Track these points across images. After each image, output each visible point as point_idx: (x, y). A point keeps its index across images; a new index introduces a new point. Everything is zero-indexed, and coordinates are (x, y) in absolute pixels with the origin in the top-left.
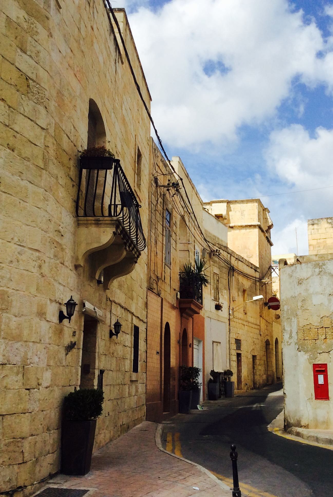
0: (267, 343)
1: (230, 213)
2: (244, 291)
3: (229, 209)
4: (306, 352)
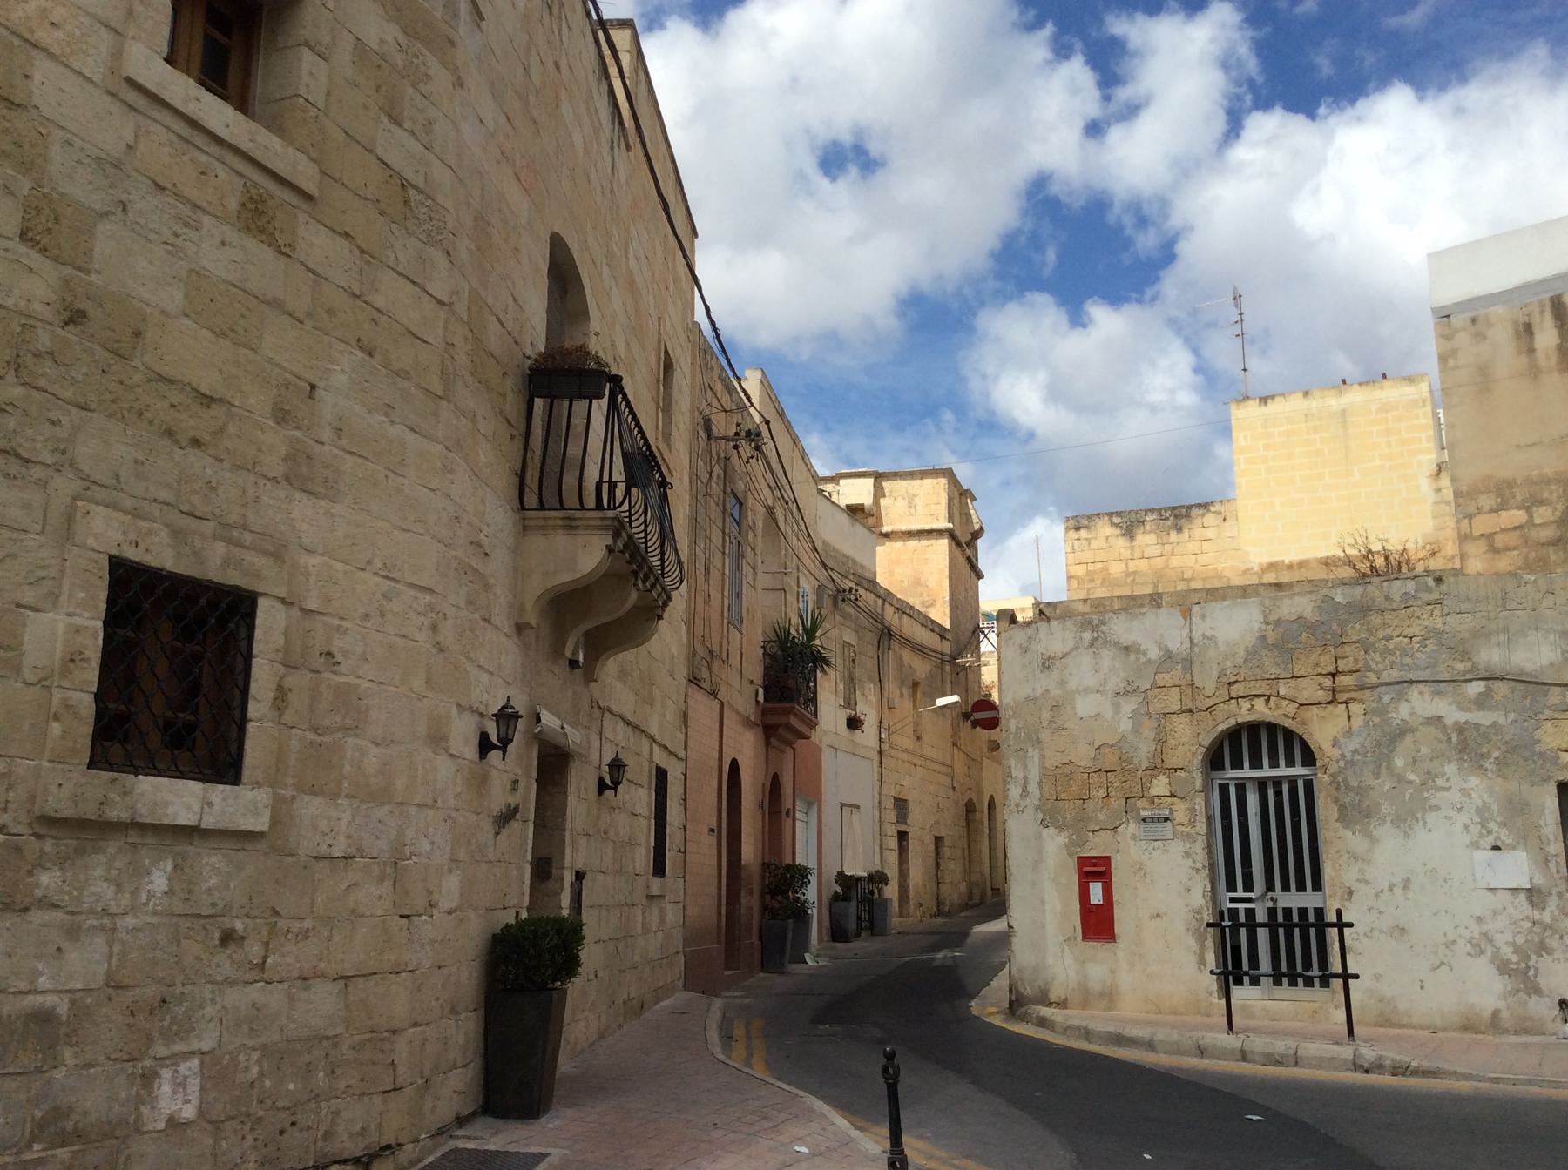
0: (970, 808)
1: (883, 502)
2: (915, 685)
3: (879, 493)
4: (1061, 828)
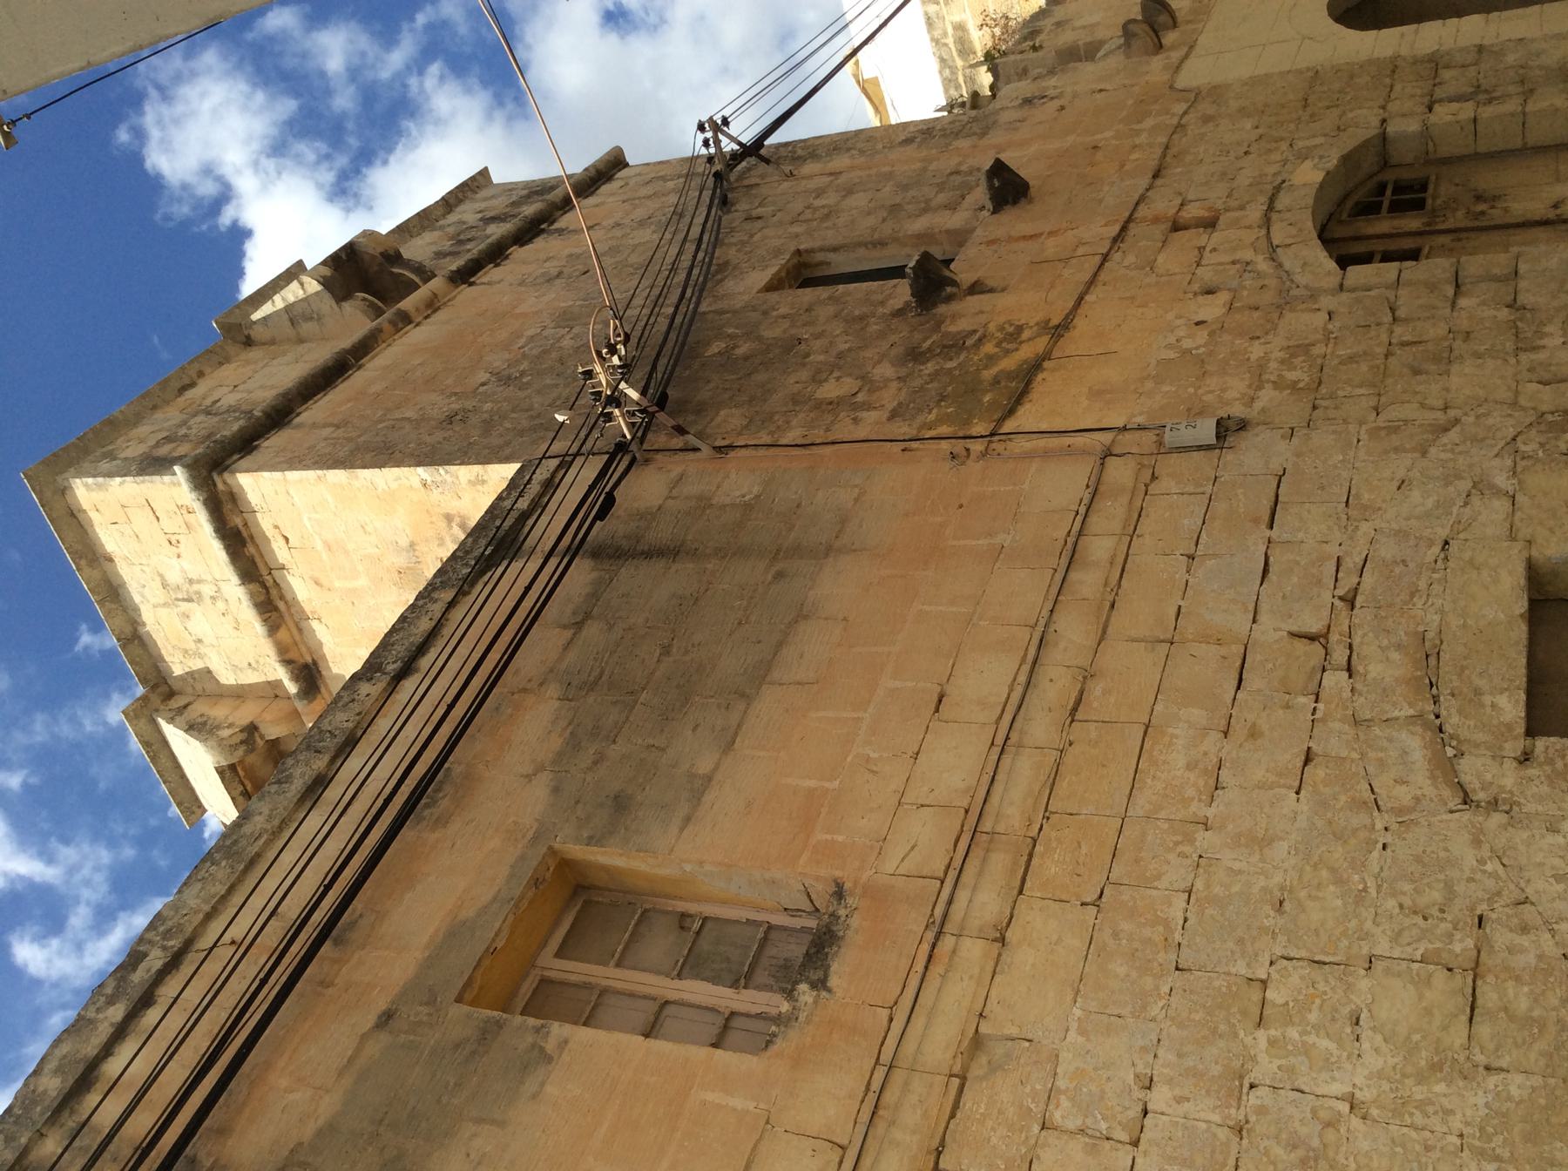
1: (227, 678)
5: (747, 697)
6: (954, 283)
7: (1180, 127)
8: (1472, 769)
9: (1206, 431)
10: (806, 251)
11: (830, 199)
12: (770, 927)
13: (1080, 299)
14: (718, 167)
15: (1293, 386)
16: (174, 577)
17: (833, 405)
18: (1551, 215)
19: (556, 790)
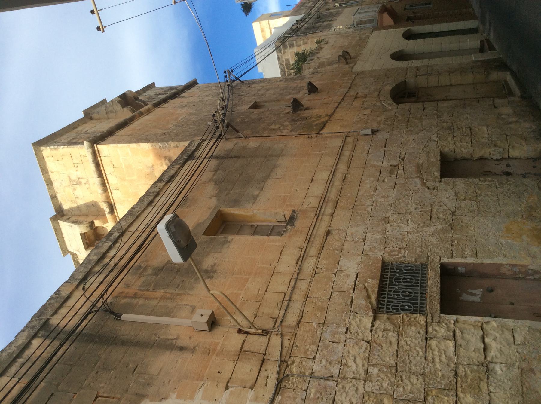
0: (402, 94)
5: (265, 182)
6: (302, 106)
7: (354, 79)
8: (430, 184)
9: (369, 131)
10: (259, 102)
11: (263, 91)
12: (274, 226)
13: (334, 111)
14: (229, 83)
15: (388, 124)
16: (74, 177)
17: (275, 130)
18: (445, 98)
19: (218, 200)
